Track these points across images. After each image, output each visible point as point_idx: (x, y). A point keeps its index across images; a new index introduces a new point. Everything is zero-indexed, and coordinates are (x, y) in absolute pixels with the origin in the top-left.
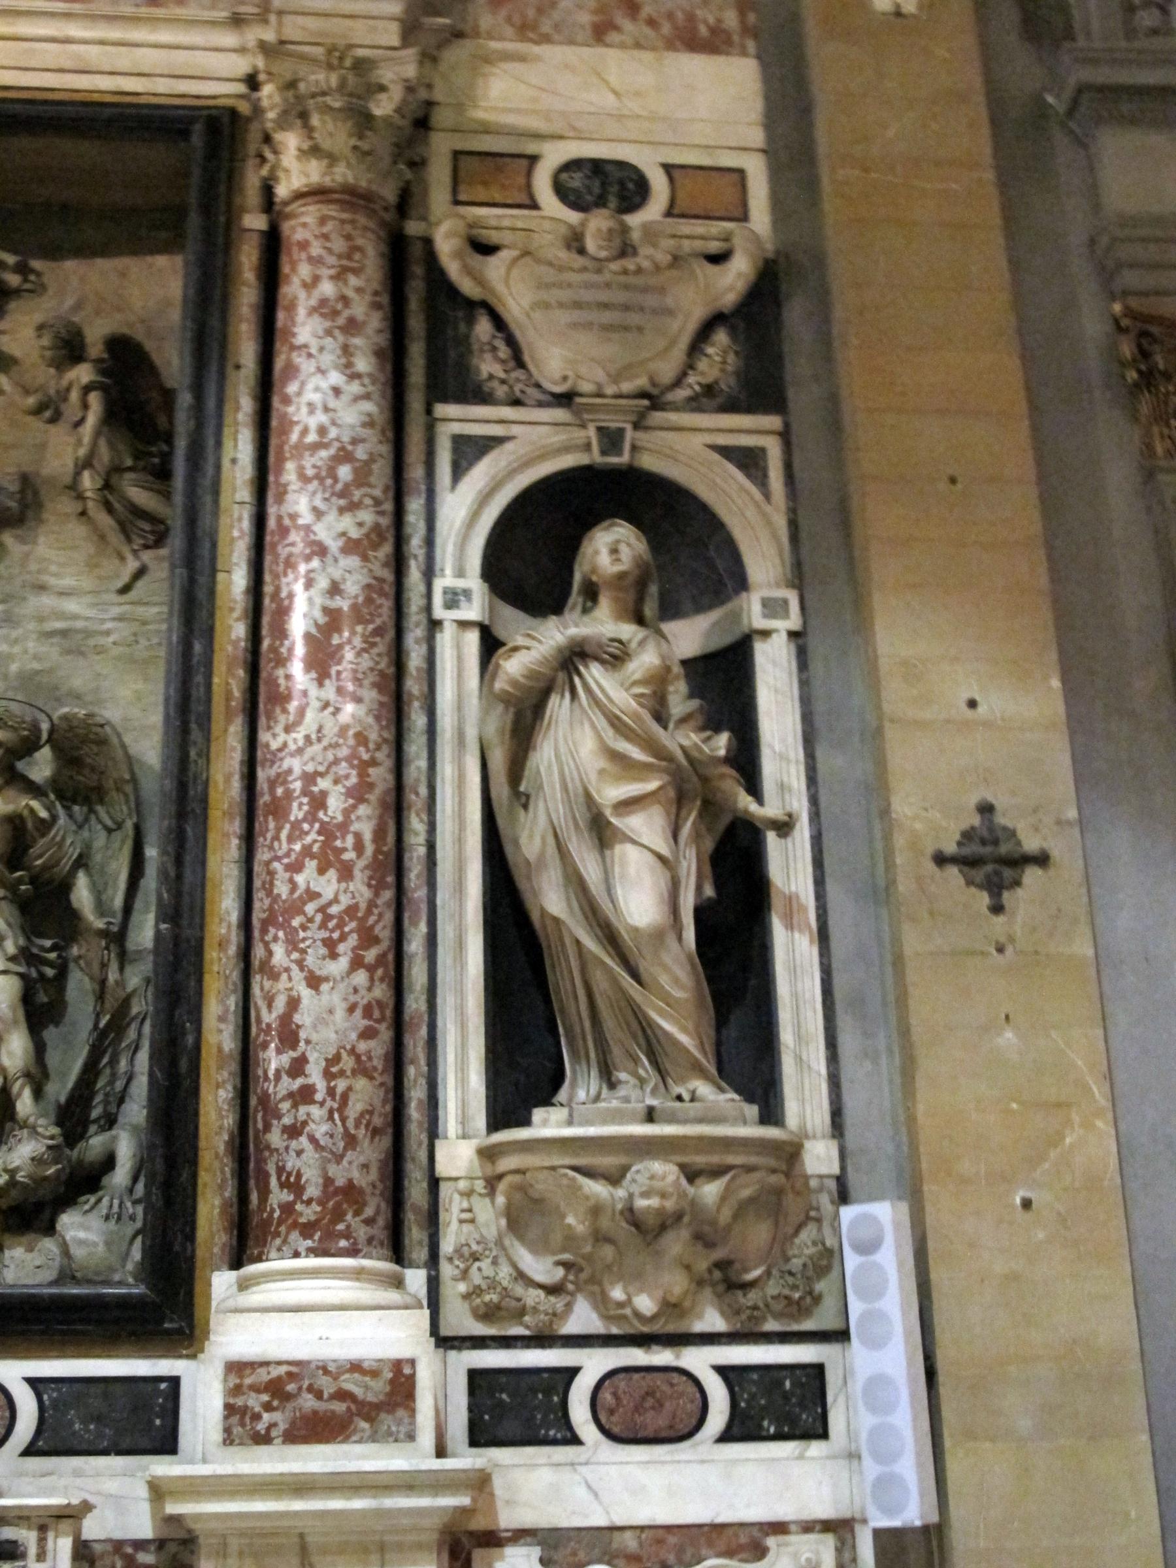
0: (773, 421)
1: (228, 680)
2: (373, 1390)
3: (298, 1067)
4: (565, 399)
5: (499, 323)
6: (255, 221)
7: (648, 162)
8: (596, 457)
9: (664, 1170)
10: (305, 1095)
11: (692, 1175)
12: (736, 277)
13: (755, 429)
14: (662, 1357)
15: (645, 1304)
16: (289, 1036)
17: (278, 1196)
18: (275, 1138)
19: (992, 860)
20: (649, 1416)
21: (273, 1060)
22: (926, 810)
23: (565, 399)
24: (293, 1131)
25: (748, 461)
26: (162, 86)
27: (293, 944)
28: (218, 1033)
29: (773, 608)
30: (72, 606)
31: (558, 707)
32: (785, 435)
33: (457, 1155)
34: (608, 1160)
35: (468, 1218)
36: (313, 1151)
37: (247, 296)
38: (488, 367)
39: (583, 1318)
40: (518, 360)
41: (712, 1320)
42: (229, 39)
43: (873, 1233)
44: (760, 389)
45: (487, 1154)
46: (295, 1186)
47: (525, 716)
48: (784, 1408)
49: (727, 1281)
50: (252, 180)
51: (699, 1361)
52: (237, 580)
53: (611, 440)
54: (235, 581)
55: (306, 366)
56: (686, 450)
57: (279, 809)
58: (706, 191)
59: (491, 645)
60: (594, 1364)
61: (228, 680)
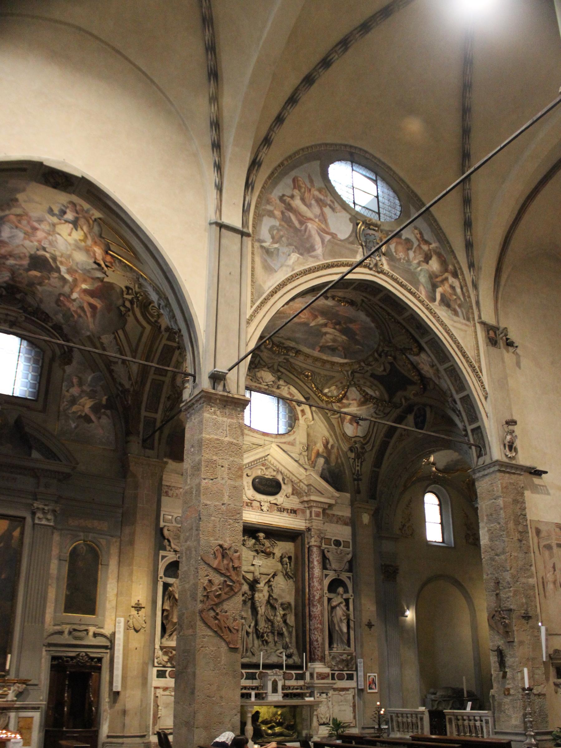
0: (351, 574)
1: (307, 602)
2: (326, 675)
3: (318, 644)
4: (335, 570)
5: (329, 560)
6: (307, 546)
7: (341, 540)
8: (337, 577)
9: (345, 656)
10: (319, 647)
11: (348, 656)
12: (350, 556)
13: (349, 574)
14: (342, 672)
15: (341, 667)
16: (317, 641)
17: (316, 657)
18: (316, 651)
19: (370, 625)
20: (341, 678)
21: (315, 643)
22: (365, 621)
23: (335, 570)
24: (318, 650)
25: (349, 578)
26: (298, 527)
27: (317, 632)
28: (308, 640)
29: (351, 596)
30: (283, 586)
31: (338, 608)
32: (353, 576)
33: (327, 652)
34: (341, 654)
35: (328, 658)
36: (319, 653)
37: (307, 556)
38: (328, 566)
39: (336, 669)
40: (330, 565)
41: (345, 669)
42: (304, 521)
43: (360, 662)
44: (350, 570)
45: (329, 653)
46: (318, 656)
47: (333, 608)
48: (350, 677)
49: (347, 665)
50: (306, 541)
51: (344, 673)
52: (307, 590)
53: (338, 576)
54: (307, 590)
55: (316, 568)
56: (344, 577)
57: (315, 618)
58: (346, 544)
59: (329, 600)
60: (337, 673)
61: (307, 602)
